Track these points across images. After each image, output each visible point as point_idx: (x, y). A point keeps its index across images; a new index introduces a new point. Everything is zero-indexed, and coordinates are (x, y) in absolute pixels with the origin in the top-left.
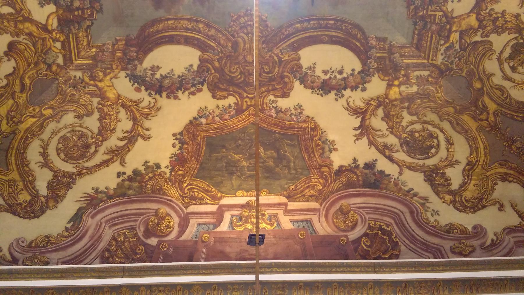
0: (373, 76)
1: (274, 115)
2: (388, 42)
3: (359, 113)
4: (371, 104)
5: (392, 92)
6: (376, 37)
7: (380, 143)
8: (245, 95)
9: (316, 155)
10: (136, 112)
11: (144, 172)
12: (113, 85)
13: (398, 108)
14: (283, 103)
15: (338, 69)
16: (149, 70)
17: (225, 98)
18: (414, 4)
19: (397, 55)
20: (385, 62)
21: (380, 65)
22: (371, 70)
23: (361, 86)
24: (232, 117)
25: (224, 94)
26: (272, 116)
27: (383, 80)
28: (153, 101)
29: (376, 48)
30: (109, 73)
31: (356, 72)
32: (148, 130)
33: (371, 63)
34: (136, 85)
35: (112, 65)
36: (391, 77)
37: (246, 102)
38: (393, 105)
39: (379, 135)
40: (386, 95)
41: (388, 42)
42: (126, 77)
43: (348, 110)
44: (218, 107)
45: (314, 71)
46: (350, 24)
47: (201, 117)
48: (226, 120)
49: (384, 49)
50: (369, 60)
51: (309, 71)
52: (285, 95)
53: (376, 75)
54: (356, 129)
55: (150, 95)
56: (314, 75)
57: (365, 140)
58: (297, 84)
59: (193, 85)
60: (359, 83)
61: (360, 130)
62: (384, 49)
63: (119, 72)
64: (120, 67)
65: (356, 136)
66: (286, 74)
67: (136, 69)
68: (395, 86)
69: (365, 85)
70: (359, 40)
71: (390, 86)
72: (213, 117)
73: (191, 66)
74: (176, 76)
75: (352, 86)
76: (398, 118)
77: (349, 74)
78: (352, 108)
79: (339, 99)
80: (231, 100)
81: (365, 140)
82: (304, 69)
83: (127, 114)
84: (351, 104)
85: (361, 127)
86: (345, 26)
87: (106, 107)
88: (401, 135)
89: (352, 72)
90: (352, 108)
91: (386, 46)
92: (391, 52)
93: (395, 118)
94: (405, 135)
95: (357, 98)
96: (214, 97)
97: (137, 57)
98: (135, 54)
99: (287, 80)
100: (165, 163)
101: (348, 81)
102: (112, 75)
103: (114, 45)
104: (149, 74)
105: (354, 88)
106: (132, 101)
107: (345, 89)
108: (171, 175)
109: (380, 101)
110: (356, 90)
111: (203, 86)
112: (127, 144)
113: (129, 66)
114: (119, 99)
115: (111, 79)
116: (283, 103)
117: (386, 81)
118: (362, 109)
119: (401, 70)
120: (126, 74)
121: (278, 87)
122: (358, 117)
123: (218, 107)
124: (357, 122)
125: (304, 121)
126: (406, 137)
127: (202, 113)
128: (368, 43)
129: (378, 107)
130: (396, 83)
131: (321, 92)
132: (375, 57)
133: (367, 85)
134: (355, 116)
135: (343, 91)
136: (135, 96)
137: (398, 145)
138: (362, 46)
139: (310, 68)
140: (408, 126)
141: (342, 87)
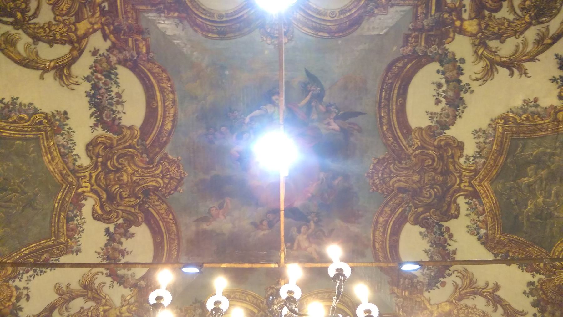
0: (447, 50)
1: (484, 160)
2: (410, 33)
3: (491, 68)
4: (482, 54)
5: (469, 29)
6: (403, 46)
7: (534, 47)
8: (456, 186)
9: (540, 122)
10: (467, 291)
11: (536, 298)
12: (437, 304)
13: (490, 23)
14: (470, 149)
15: (436, 88)
16: (423, 271)
17: (458, 207)
18: (373, 9)
19: (425, 22)
20: (432, 36)
21: (435, 41)
22: (440, 52)
23: (458, 64)
24: (481, 203)
25: (453, 207)
26: (484, 163)
27: (453, 39)
28: (456, 273)
29: (415, 47)
30: (424, 304)
31: (441, 69)
32: (487, 284)
33: (431, 52)
34: (438, 285)
35: (416, 301)
36: (451, 30)
37: (465, 186)
38: (485, 28)
39: (523, 48)
40: (473, 35)
41: (410, 33)
42: (429, 292)
43: (487, 81)
44: (467, 215)
45: (435, 114)
46: (386, 76)
47: (478, 233)
48: (484, 210)
49: (417, 37)
50: (429, 54)
51: (435, 119)
52: (460, 146)
53: (447, 46)
54: (512, 74)
55: (449, 275)
56: (441, 114)
57: (527, 65)
58: (448, 133)
59: (442, 234)
60: (454, 66)
62: (417, 37)
63: (424, 297)
64: (419, 295)
66: (436, 143)
67: (421, 282)
68: (461, 25)
69: (457, 60)
70: (405, 65)
71: (461, 31)
72: (479, 221)
73: (421, 233)
74: (431, 248)
75: (457, 73)
76: (503, 24)
77: (442, 76)
78: (485, 75)
79: (471, 89)
80: (461, 201)
81: (527, 65)
82: (433, 124)
83: (468, 299)
84: (479, 76)
85: (509, 68)
86: (388, 80)
87: (459, 314)
88: (526, 22)
89: (440, 73)
90: (485, 75)
91: (413, 35)
92: (421, 30)
93: (503, 27)
94: (527, 17)
95: (472, 69)
96: (456, 217)
97: (410, 279)
98: (407, 280)
99: (442, 143)
100: (528, 277)
101: (451, 77)
102: (427, 303)
103: (398, 297)
104: (427, 272)
105: (460, 71)
106: (455, 291)
107: (459, 82)
108: (543, 274)
109: (480, 44)
110: (462, 70)
111: (443, 226)
112: (501, 306)
113: (418, 287)
114: (452, 302)
115: (430, 304)
116: (470, 149)
117: (454, 35)
118: (487, 65)
119: (443, 17)
120: (426, 291)
121: (450, 153)
122: (497, 70)
123: (467, 215)
124: (503, 72)
125: (495, 129)
126: (530, 16)
127: (474, 231)
128: (409, 55)
129: (486, 47)
130: (458, 23)
131: (461, 108)
132: (425, 47)
133: (458, 57)
134: (495, 73)
135: (461, 84)
136: (449, 288)
137: (539, 27)
138: (411, 61)
139: (431, 118)
140: (515, 13)
141: (457, 84)
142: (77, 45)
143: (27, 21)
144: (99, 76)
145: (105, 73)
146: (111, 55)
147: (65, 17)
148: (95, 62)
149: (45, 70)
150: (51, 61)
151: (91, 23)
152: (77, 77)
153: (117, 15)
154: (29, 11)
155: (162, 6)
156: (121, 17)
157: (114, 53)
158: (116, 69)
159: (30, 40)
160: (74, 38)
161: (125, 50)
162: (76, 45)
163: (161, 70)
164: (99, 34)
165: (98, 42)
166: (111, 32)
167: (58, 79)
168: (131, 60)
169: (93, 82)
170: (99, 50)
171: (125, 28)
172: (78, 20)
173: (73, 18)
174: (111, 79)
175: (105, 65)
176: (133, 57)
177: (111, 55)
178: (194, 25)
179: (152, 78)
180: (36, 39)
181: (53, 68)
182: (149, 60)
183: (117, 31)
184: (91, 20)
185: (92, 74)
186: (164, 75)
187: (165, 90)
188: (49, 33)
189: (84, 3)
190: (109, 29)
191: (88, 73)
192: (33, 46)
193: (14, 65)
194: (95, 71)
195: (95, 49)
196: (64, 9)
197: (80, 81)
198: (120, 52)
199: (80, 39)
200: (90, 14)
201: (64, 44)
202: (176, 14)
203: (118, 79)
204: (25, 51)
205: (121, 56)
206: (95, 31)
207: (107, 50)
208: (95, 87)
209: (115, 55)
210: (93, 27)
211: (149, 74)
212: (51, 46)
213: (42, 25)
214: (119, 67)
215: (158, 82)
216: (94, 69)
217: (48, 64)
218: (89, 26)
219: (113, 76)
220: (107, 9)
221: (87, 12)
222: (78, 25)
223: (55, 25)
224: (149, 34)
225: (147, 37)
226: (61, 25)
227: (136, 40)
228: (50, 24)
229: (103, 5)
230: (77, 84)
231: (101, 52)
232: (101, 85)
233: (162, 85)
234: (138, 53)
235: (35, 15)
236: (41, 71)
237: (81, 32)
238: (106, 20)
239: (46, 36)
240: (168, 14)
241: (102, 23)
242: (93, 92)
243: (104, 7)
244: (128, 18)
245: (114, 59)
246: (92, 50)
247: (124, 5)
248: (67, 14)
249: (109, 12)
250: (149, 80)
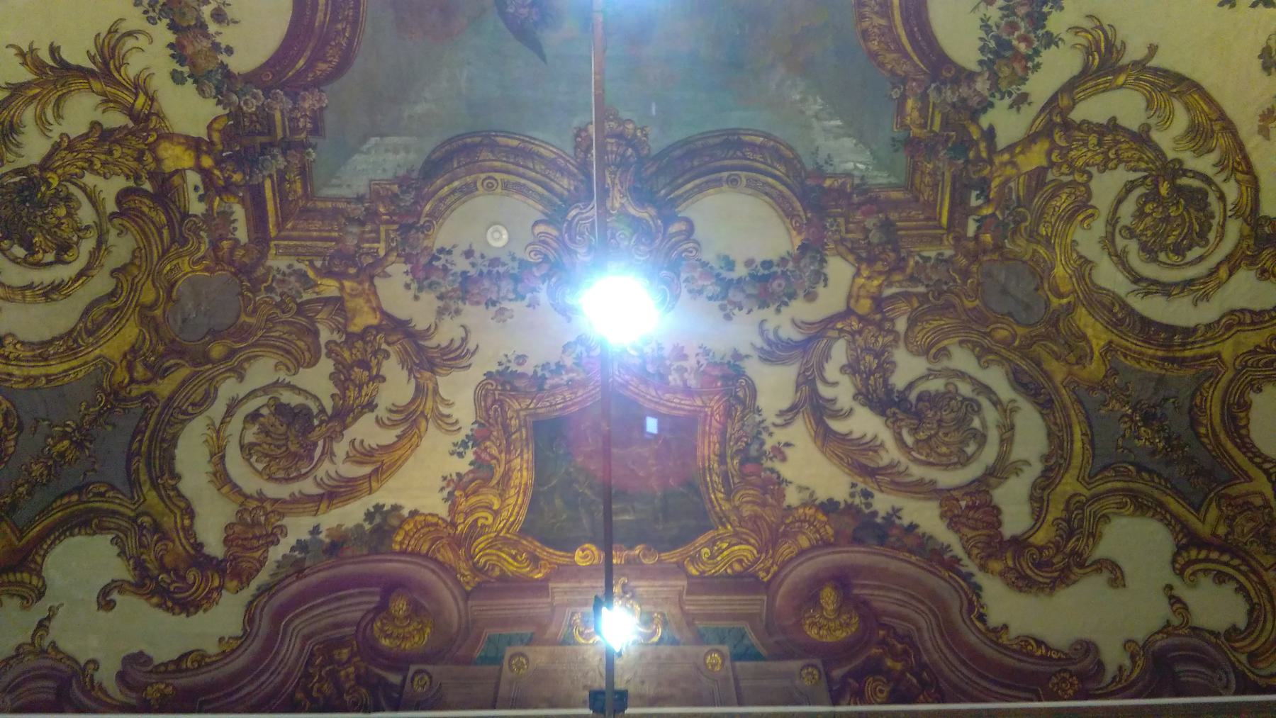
0: (219, 103)
2: (312, 140)
3: (106, 64)
4: (137, 95)
5: (179, 150)
6: (322, 109)
7: (20, 116)
13: (133, 164)
15: (226, 9)
18: (404, 192)
19: (281, 162)
20: (260, 134)
21: (252, 122)
22: (235, 98)
23: (186, 70)
27: (209, 127)
29: (294, 109)
31: (223, 57)
33: (255, 97)
36: (220, 147)
38: (142, 153)
39: (43, 112)
40: (170, 137)
41: (312, 140)
43: (109, 32)
46: (350, 42)
49: (295, 130)
50: (260, 92)
53: (220, 110)
54: (54, 51)
57: (24, 75)
60: (193, 65)
61: (52, 63)
62: (295, 130)
65: (32, 50)
68: (198, 158)
69: (190, 80)
70: (310, 65)
71: (195, 145)
75: (183, 47)
76: (104, 164)
77: (218, 39)
78: (115, 46)
79: (141, 9)
81: (24, 75)
84: (130, 43)
85: (65, 66)
86: (344, 30)
88: (54, 171)
89: (223, 46)
90: (115, 46)
91: (303, 136)
92: (287, 146)
93: (103, 157)
94: (55, 182)
95: (151, 56)
101: (195, 37)
105: (178, 52)
107: (173, 27)
109: (147, 118)
110: (173, 56)
117: (210, 136)
118: (119, 72)
119: (244, 174)
122: (92, 59)
124: (76, 55)
126: (49, 185)
128: (306, 89)
129: (130, 111)
130: (207, 162)
132: (271, 108)
133: (190, 85)
134: (93, 51)
135: (168, 21)
137: (22, 163)
138: (300, 74)
140: (83, 189)
141: (177, 20)
142: (1056, 121)
143: (1150, 175)
144: (1022, 47)
145: (1008, 54)
146: (986, 93)
147: (1065, 179)
148: (1024, 80)
149: (1140, 66)
150: (1121, 87)
151: (1013, 163)
152: (1074, 46)
153: (954, 179)
154: (1141, 196)
155: (855, 199)
156: (948, 176)
157: (977, 99)
158: (981, 63)
159: (1156, 136)
160: (1058, 137)
161: (954, 105)
162: (1058, 120)
163: (880, 58)
164: (1002, 141)
165: (1008, 123)
166: (976, 143)
167: (1118, 44)
168: (944, 83)
169: (1040, 32)
170: (1011, 107)
171: (942, 154)
172: (1040, 173)
173: (1050, 177)
174: (997, 39)
175: (1006, 71)
176: (939, 90)
177: (986, 93)
178: (791, 162)
179: (904, 40)
180: (1142, 138)
181: (1122, 70)
182: (904, 80)
183: (965, 144)
184: (1014, 171)
185: (1037, 52)
186: (874, 45)
187: (877, 8)
188: (1109, 149)
189: (1018, 206)
190: (978, 152)
191: (1047, 56)
192: (1153, 121)
193: (1205, 84)
194: (1029, 58)
195: (1019, 109)
196: (1064, 197)
197: (1068, 37)
198: (964, 100)
199: (1046, 132)
200: (1012, 184)
201: (1084, 122)
202: (828, 183)
203: (981, 39)
204: (1172, 112)
205: (964, 91)
206: (1010, 148)
207: (992, 105)
208: (1038, 20)
209: (978, 93)
210: (1013, 156)
211: (909, 48)
212: (1114, 119)
213: (1122, 166)
214: (974, 67)
215: (891, 28)
216: (1030, 64)
217: (1131, 80)
218: (1020, 159)
219: (992, 44)
220: (974, 194)
221: (1018, 188)
222: (1045, 163)
223: (1093, 165)
224: (893, 139)
225: (898, 133)
226: (1080, 163)
227: (924, 126)
228: (1104, 167)
229: (980, 202)
230: (1076, 30)
231: (1007, 101)
232: (1022, 24)
233: (883, 22)
234: (924, 97)
235: (1130, 187)
236: (1153, 63)
237: (1041, 147)
238: (979, 171)
239: (1119, 142)
240: (844, 184)
241: (991, 162)
242: (1045, 9)
243: (978, 197)
244: (933, 174)
245: (982, 85)
246: (1024, 107)
247: (935, 200)
248: (1062, 186)
249: (969, 187)
250: (910, 35)
